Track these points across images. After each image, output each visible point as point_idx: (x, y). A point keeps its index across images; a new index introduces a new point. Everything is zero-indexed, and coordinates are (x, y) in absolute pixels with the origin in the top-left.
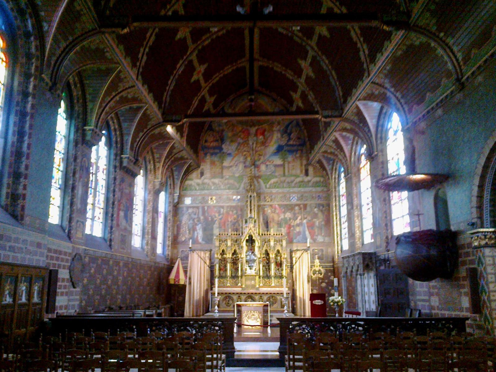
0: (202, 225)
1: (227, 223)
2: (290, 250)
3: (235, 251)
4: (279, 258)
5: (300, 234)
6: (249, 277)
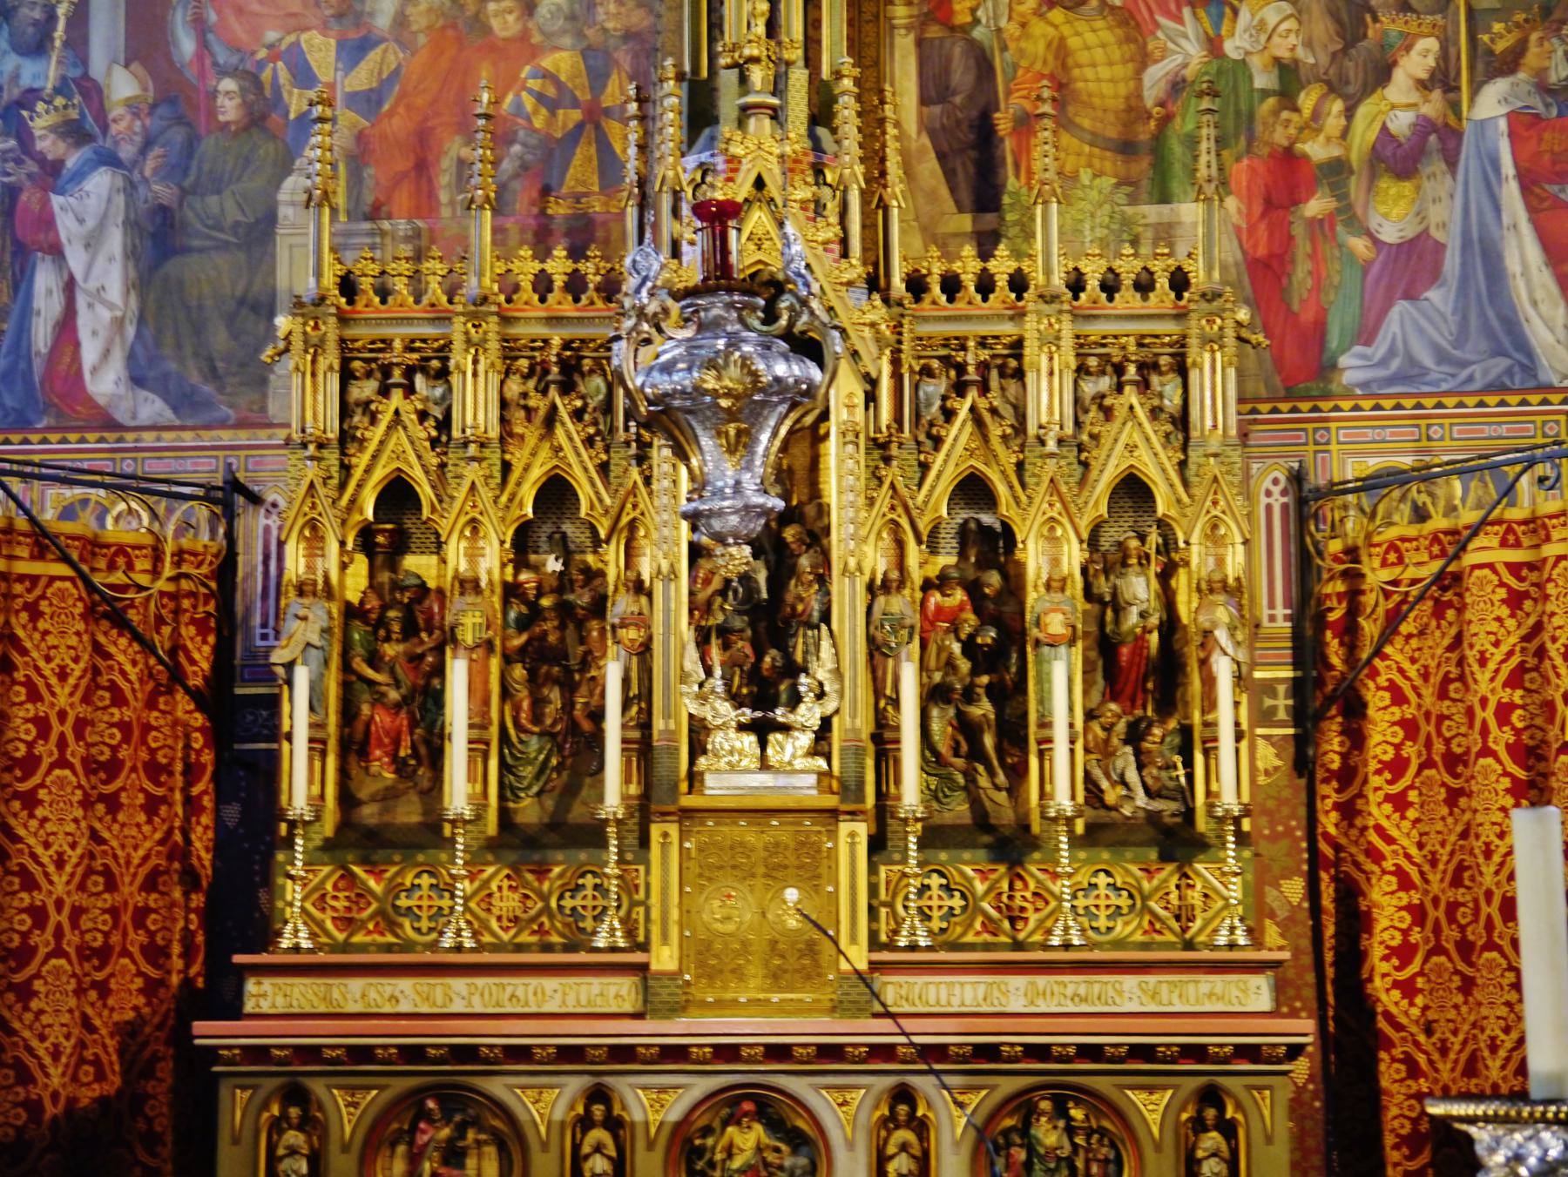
0: (130, 188)
1: (455, 149)
2: (1297, 478)
3: (556, 494)
4: (1140, 588)
5: (1434, 275)
6: (743, 832)
